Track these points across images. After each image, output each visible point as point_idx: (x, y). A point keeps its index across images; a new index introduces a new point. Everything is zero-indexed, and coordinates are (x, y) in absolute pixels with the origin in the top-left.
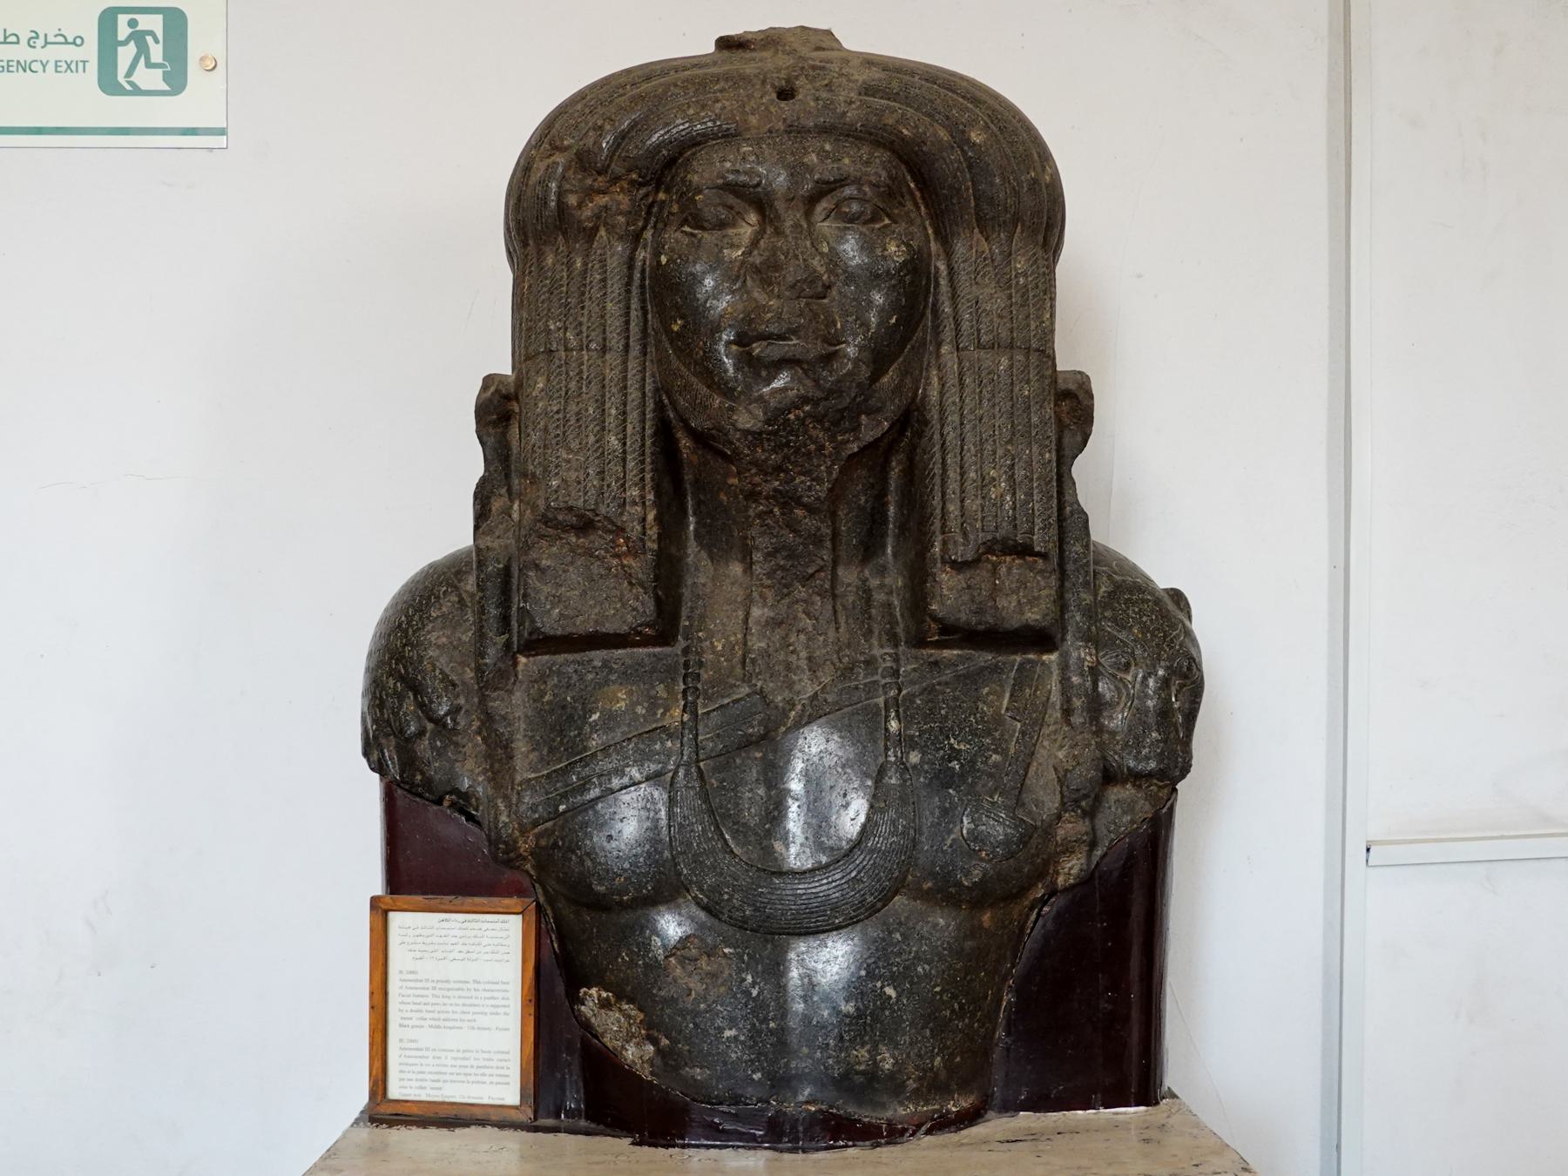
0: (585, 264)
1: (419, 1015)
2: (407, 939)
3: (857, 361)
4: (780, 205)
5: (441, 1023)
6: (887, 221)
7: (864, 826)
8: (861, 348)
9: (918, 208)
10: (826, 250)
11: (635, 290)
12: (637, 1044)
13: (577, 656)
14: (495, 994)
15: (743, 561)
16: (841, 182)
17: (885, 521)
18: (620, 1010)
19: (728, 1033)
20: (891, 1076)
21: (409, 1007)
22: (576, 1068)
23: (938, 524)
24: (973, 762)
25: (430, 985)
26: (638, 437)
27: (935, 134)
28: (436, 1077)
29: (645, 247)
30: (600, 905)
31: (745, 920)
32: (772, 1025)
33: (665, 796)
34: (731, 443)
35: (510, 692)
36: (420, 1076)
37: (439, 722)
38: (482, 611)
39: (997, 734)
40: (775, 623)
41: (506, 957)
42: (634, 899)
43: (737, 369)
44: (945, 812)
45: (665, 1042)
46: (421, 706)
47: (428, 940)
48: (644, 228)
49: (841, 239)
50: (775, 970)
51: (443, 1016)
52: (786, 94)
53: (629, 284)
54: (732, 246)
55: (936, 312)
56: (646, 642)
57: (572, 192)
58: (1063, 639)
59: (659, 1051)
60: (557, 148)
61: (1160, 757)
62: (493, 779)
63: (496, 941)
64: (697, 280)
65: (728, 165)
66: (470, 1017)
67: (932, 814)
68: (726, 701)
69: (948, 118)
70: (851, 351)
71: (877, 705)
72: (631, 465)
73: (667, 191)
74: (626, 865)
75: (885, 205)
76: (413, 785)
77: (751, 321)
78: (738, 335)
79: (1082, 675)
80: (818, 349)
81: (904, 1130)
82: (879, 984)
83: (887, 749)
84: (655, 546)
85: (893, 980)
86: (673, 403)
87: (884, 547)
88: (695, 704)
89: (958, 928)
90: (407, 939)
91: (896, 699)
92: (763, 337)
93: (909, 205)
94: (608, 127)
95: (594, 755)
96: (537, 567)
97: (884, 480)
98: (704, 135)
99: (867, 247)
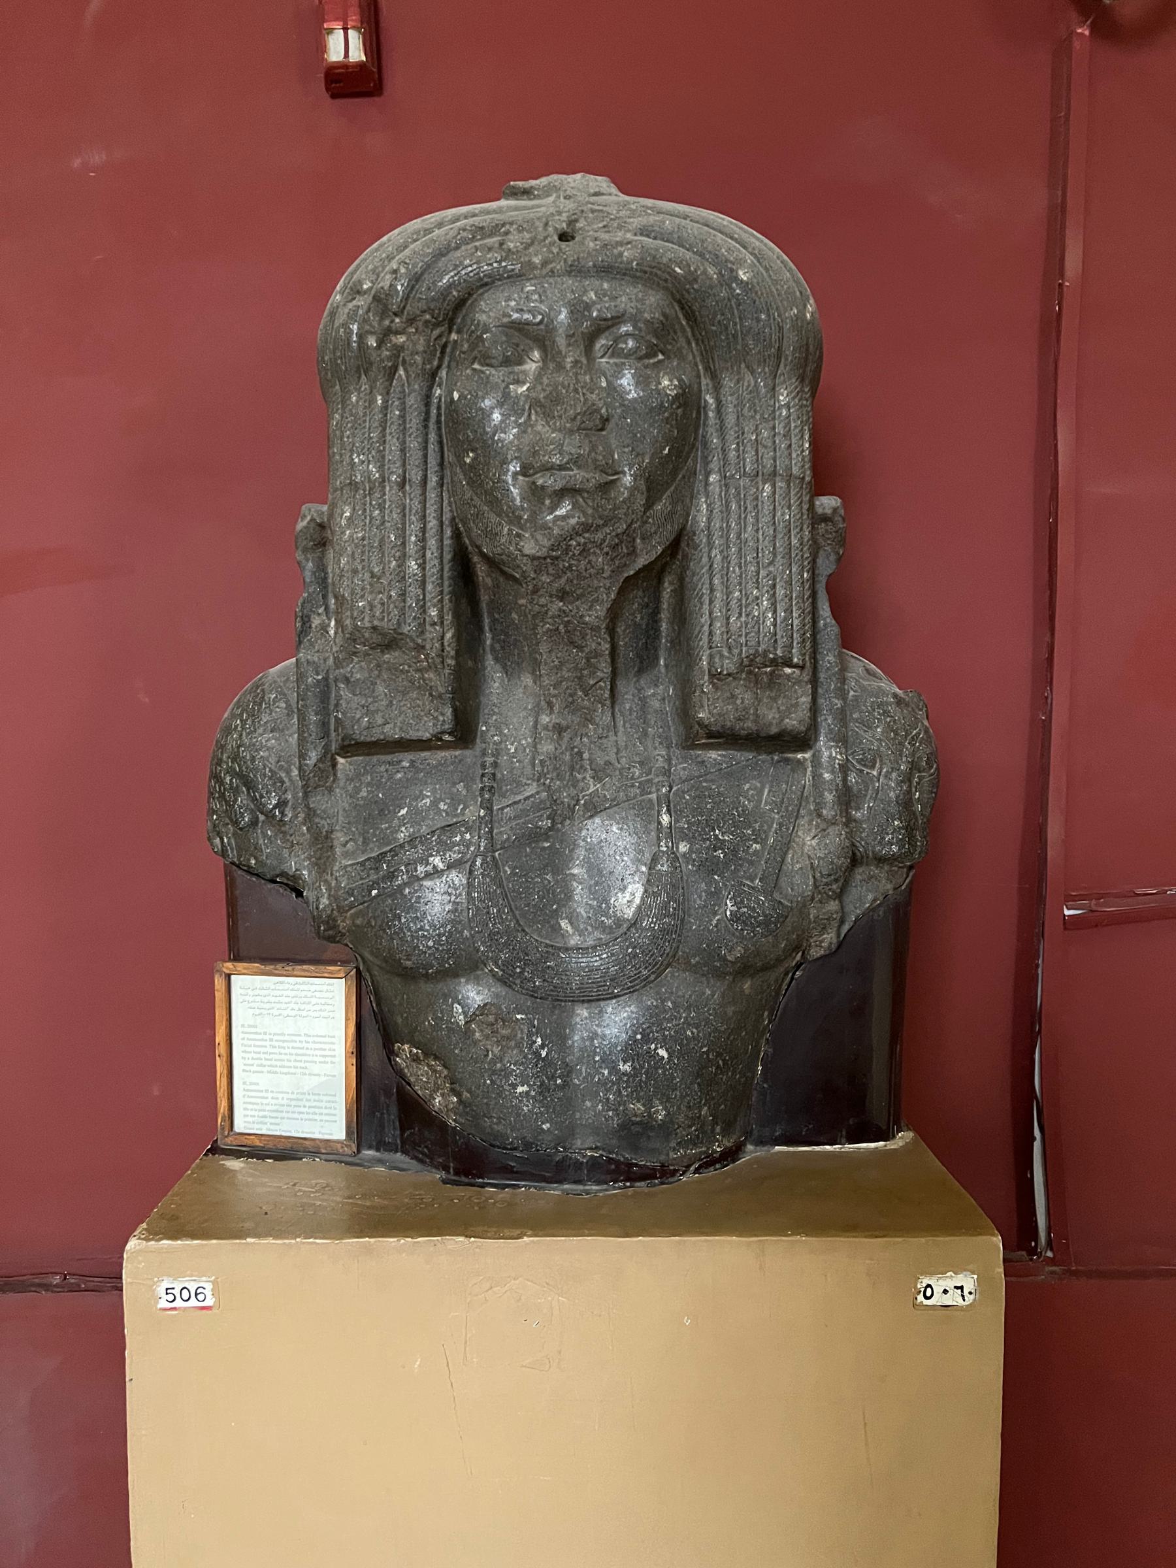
0: (385, 401)
1: (259, 1062)
2: (247, 998)
3: (633, 490)
4: (561, 342)
5: (278, 1069)
6: (661, 357)
7: (639, 908)
8: (635, 476)
9: (689, 343)
10: (604, 384)
11: (432, 425)
12: (443, 1095)
13: (388, 758)
15: (533, 673)
16: (618, 320)
17: (657, 637)
18: (428, 1065)
19: (520, 1089)
20: (663, 1125)
21: (250, 1056)
22: (394, 1109)
23: (705, 638)
24: (735, 852)
25: (267, 1037)
26: (436, 562)
27: (705, 272)
28: (275, 1114)
29: (440, 385)
30: (409, 975)
31: (535, 989)
32: (559, 1081)
33: (464, 881)
34: (518, 566)
35: (330, 790)
36: (261, 1114)
37: (269, 815)
38: (302, 718)
39: (757, 826)
40: (559, 729)
42: (437, 972)
43: (523, 499)
44: (711, 895)
45: (466, 1095)
46: (254, 799)
47: (265, 1000)
48: (439, 367)
49: (618, 374)
50: (559, 1036)
51: (279, 1063)
52: (564, 237)
53: (427, 419)
54: (518, 382)
55: (705, 445)
56: (447, 746)
57: (372, 333)
58: (816, 740)
59: (460, 1101)
60: (358, 292)
61: (900, 843)
62: (316, 864)
63: (323, 1001)
64: (486, 415)
65: (513, 303)
66: (302, 1065)
67: (700, 897)
68: (518, 798)
69: (717, 256)
70: (628, 479)
71: (650, 800)
72: (429, 587)
73: (459, 332)
74: (431, 943)
75: (658, 343)
76: (249, 867)
77: (535, 453)
78: (523, 467)
79: (832, 772)
80: (597, 478)
81: (676, 1171)
82: (653, 1046)
83: (659, 840)
84: (453, 662)
85: (664, 1043)
86: (468, 530)
87: (657, 658)
88: (490, 801)
89: (723, 995)
90: (247, 998)
91: (667, 795)
92: (549, 468)
93: (682, 342)
94: (403, 270)
95: (402, 846)
96: (347, 680)
97: (658, 600)
98: (489, 276)
99: (641, 381)
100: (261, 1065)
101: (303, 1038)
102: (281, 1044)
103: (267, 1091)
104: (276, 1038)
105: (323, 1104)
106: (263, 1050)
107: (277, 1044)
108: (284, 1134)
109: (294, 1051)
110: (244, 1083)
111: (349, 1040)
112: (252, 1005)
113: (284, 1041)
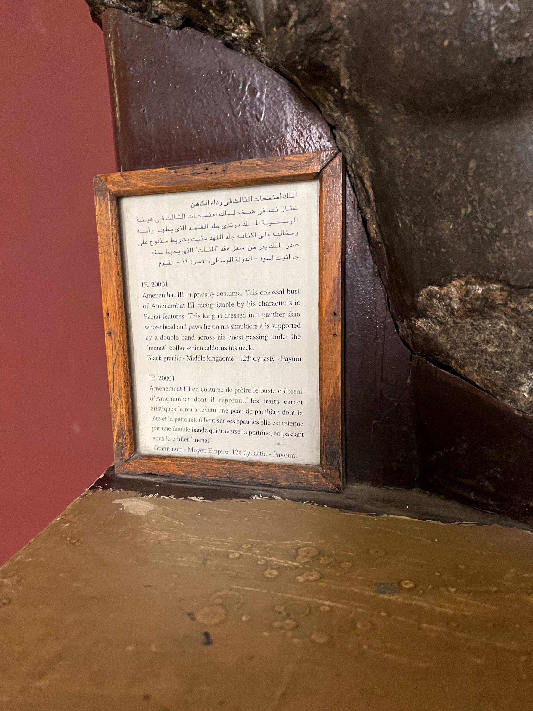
1: (173, 343)
5: (204, 354)
14: (279, 309)
21: (159, 333)
25: (185, 300)
41: (293, 252)
51: (206, 343)
63: (277, 229)
66: (243, 343)
100: (177, 348)
101: (244, 299)
102: (207, 311)
103: (187, 389)
104: (198, 300)
105: (280, 408)
106: (178, 322)
107: (199, 311)
108: (216, 456)
109: (229, 322)
110: (151, 378)
111: (328, 292)
112: (158, 248)
113: (211, 306)
